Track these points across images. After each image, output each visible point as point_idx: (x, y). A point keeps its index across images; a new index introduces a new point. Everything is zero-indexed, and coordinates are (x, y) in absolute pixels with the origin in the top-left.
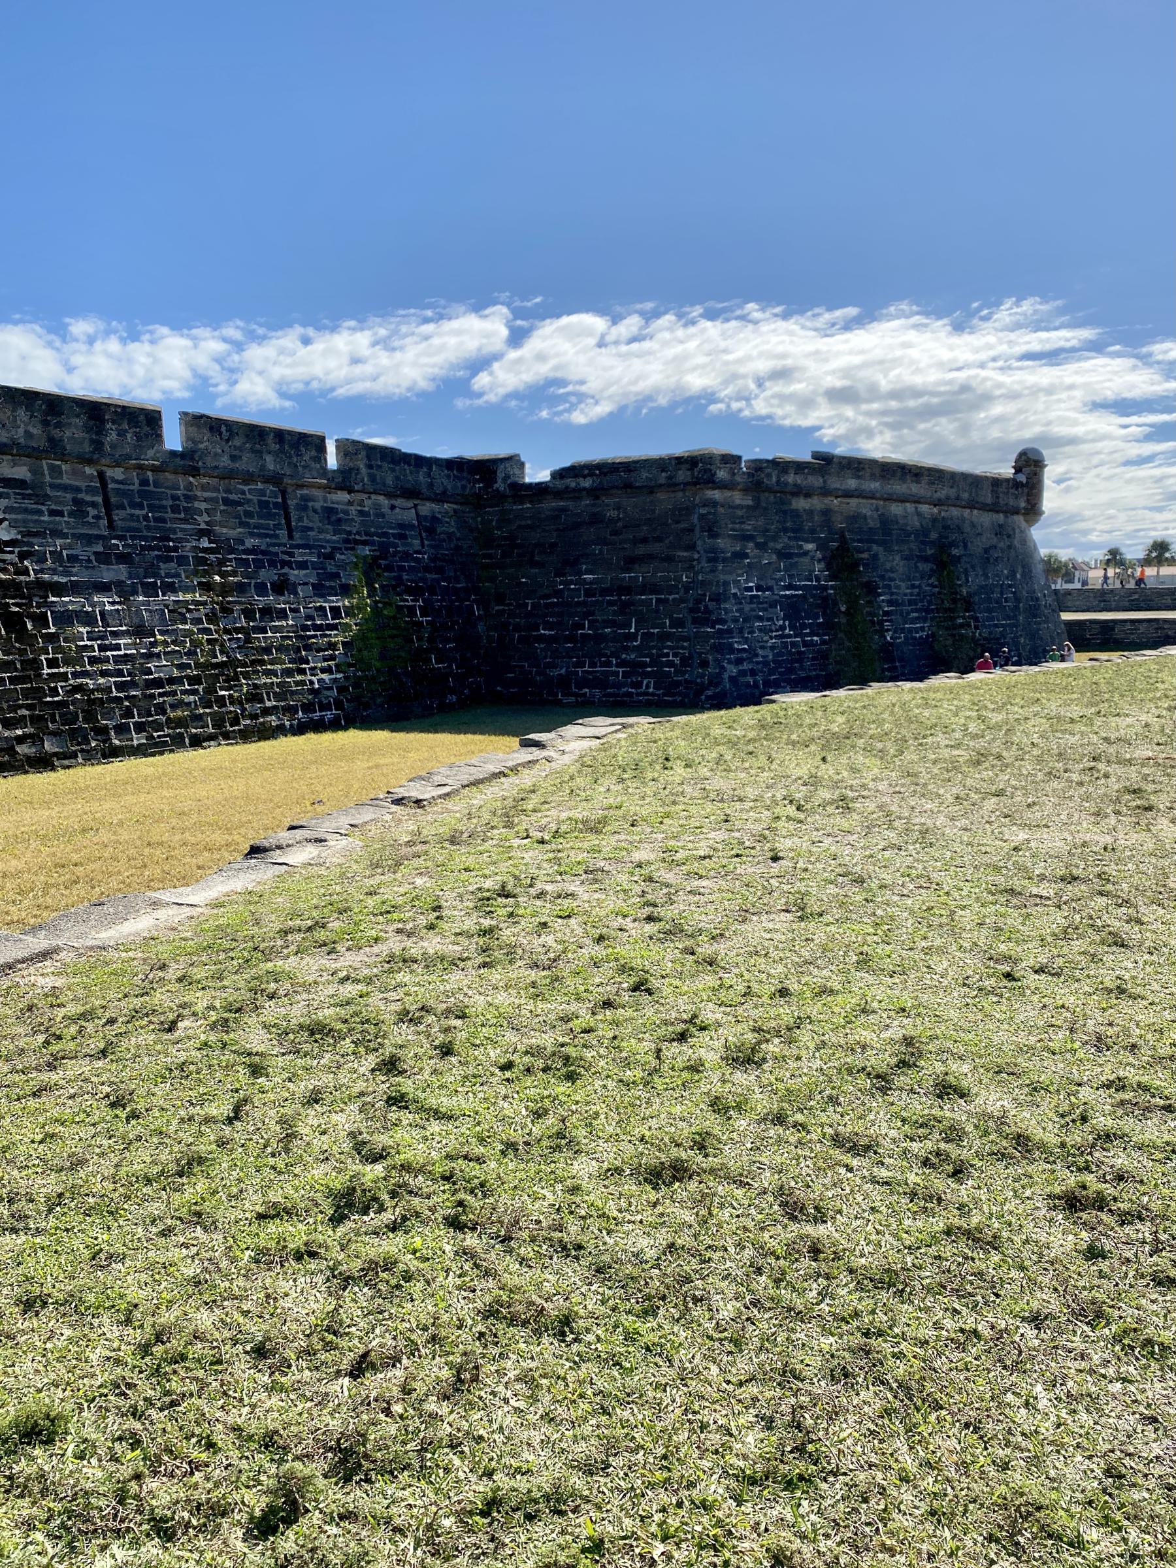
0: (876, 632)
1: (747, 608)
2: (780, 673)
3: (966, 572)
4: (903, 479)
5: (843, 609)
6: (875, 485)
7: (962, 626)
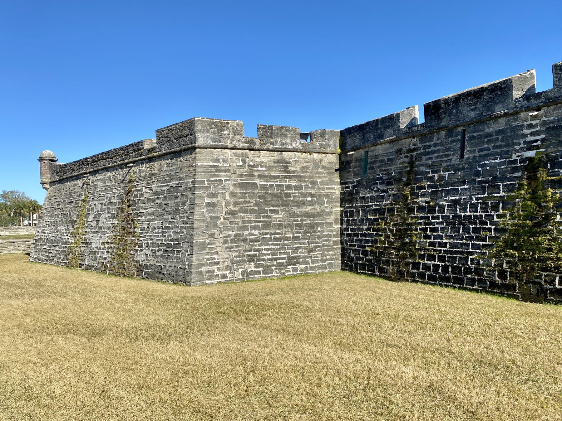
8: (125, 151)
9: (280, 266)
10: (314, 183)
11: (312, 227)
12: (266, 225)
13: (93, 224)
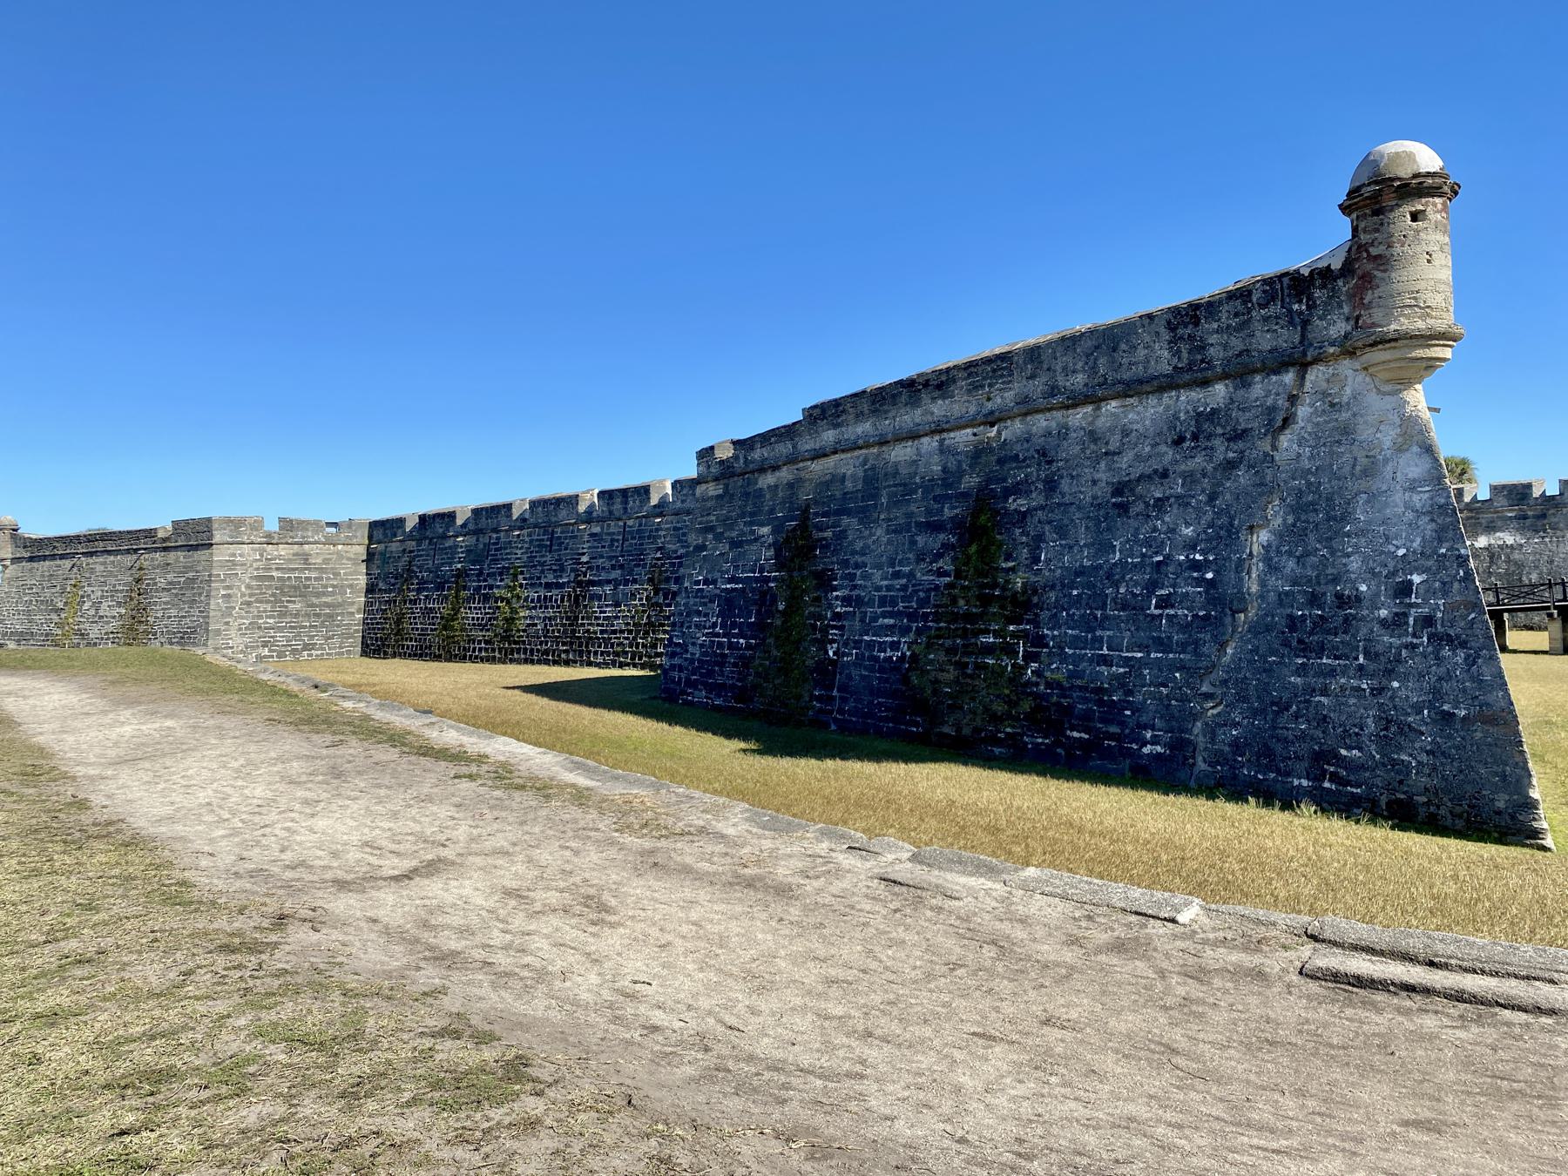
2: (701, 675)
3: (1039, 539)
4: (914, 402)
5: (781, 607)
6: (864, 428)
7: (989, 650)
8: (134, 535)
9: (294, 652)
10: (336, 574)
11: (330, 616)
12: (282, 615)
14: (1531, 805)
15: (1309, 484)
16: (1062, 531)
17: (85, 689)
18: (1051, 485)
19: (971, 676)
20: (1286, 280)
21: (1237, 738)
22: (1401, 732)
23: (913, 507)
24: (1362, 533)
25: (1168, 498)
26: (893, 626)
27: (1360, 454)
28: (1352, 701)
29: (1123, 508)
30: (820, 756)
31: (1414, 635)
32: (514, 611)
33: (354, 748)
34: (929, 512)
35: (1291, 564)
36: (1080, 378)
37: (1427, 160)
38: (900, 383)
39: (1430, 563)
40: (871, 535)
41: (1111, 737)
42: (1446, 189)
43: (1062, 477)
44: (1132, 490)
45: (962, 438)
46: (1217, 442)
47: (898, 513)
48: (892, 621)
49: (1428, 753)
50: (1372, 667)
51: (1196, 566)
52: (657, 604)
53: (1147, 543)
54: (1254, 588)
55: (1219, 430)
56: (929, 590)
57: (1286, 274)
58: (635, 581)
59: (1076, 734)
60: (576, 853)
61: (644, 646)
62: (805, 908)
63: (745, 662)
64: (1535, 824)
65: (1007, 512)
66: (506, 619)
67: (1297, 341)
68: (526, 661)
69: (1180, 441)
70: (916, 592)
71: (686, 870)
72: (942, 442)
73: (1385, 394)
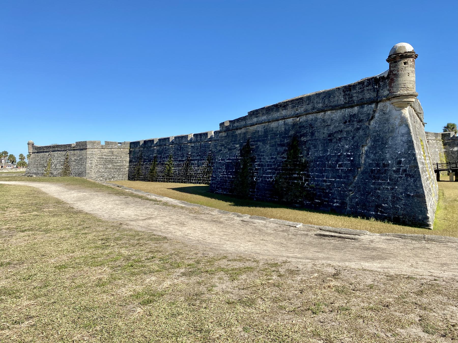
0: (250, 176)
1: (218, 165)
3: (309, 148)
4: (277, 110)
5: (242, 167)
6: (264, 118)
7: (295, 178)
13: (54, 167)
14: (427, 218)
15: (378, 134)
16: (315, 146)
17: (61, 186)
18: (313, 134)
19: (291, 186)
20: (373, 79)
21: (357, 201)
22: (397, 200)
23: (277, 140)
24: (390, 147)
25: (342, 138)
26: (271, 172)
27: (391, 126)
28: (386, 192)
29: (331, 140)
30: (249, 206)
31: (402, 175)
32: (170, 168)
33: (130, 198)
34: (281, 141)
35: (372, 155)
36: (321, 105)
37: (409, 48)
38: (274, 105)
39: (406, 155)
40: (266, 147)
41: (326, 201)
42: (413, 56)
43: (315, 132)
44: (333, 136)
45: (290, 121)
46: (355, 123)
47: (273, 141)
48: (271, 171)
49: (404, 205)
50: (391, 183)
51: (348, 156)
52: (210, 166)
53: (336, 150)
54: (363, 162)
55: (356, 120)
56: (280, 162)
57: (373, 78)
58: (203, 160)
59: (317, 201)
60: (180, 216)
61: (206, 178)
62: (224, 225)
63: (232, 182)
64: (428, 223)
65: (301, 141)
66: (168, 170)
67: (376, 96)
68: (174, 182)
69: (345, 123)
70: (277, 163)
71: (202, 219)
72: (284, 122)
73: (397, 110)
